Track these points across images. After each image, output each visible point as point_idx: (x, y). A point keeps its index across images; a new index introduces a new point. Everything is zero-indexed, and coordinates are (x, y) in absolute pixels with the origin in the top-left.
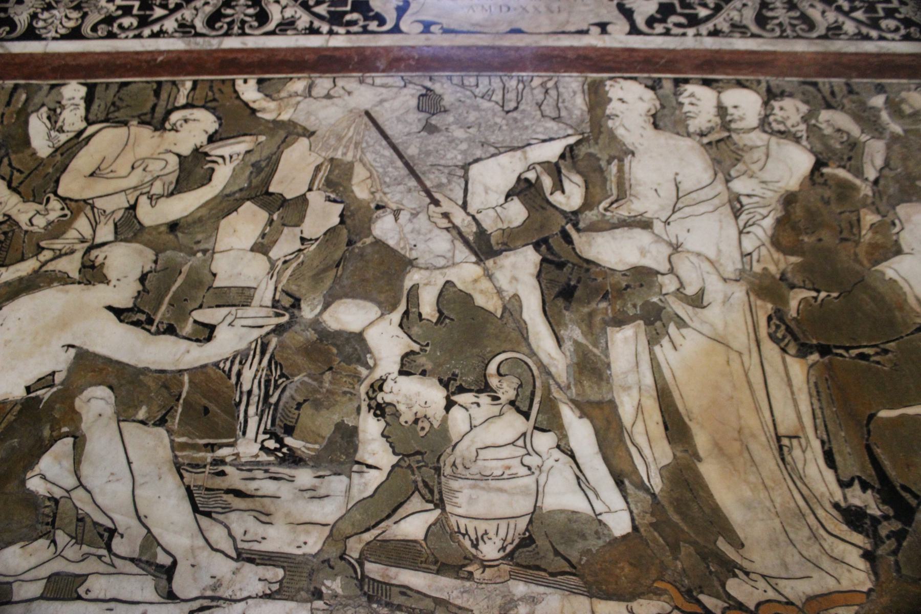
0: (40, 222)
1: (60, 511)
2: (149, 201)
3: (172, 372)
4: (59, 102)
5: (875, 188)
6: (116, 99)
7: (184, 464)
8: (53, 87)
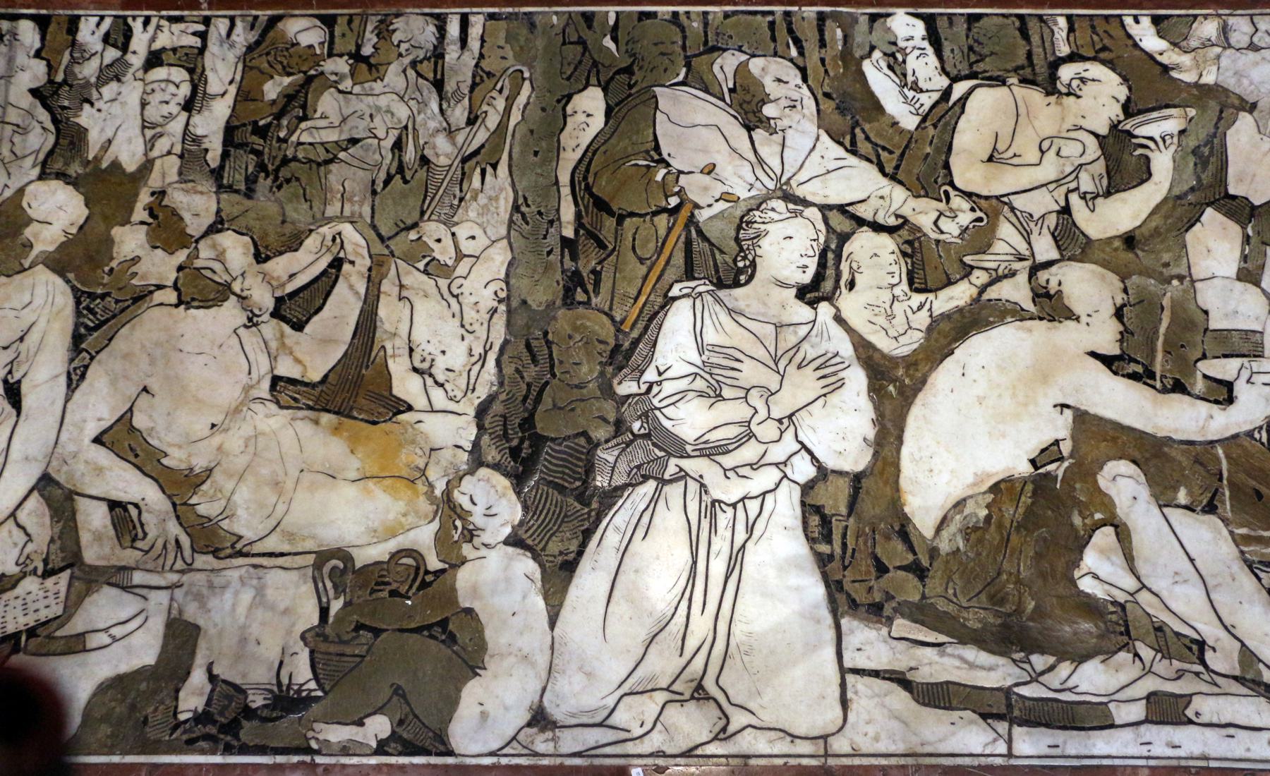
0: (951, 228)
1: (1130, 618)
2: (1083, 202)
3: (1201, 443)
4: (895, 44)
6: (971, 41)
7: (1253, 562)
8: (873, 18)
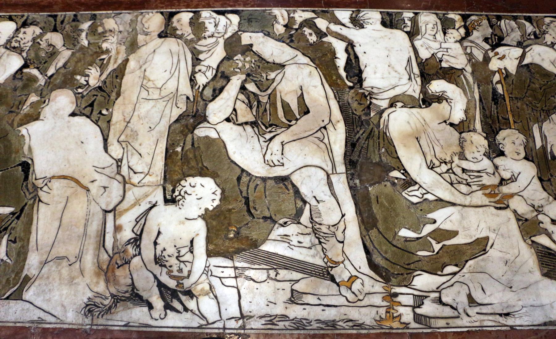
5: (49, 80)
